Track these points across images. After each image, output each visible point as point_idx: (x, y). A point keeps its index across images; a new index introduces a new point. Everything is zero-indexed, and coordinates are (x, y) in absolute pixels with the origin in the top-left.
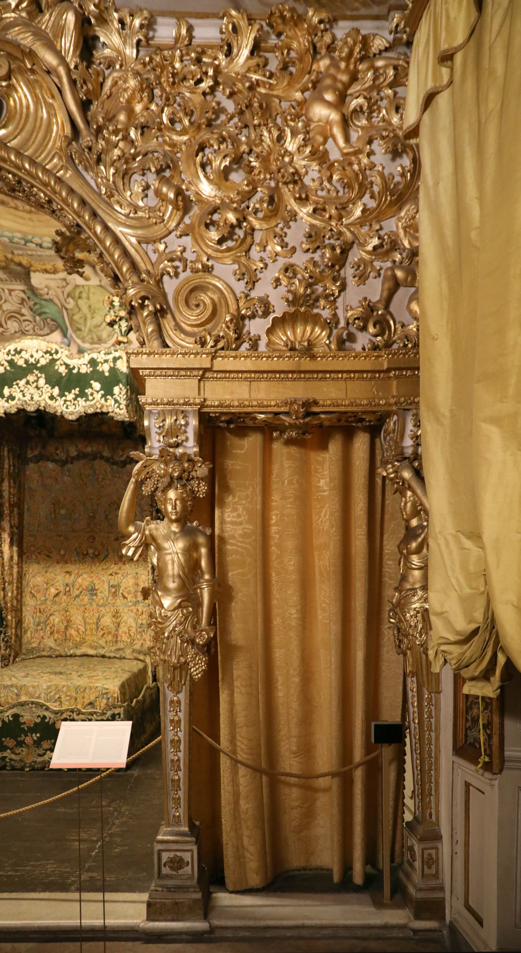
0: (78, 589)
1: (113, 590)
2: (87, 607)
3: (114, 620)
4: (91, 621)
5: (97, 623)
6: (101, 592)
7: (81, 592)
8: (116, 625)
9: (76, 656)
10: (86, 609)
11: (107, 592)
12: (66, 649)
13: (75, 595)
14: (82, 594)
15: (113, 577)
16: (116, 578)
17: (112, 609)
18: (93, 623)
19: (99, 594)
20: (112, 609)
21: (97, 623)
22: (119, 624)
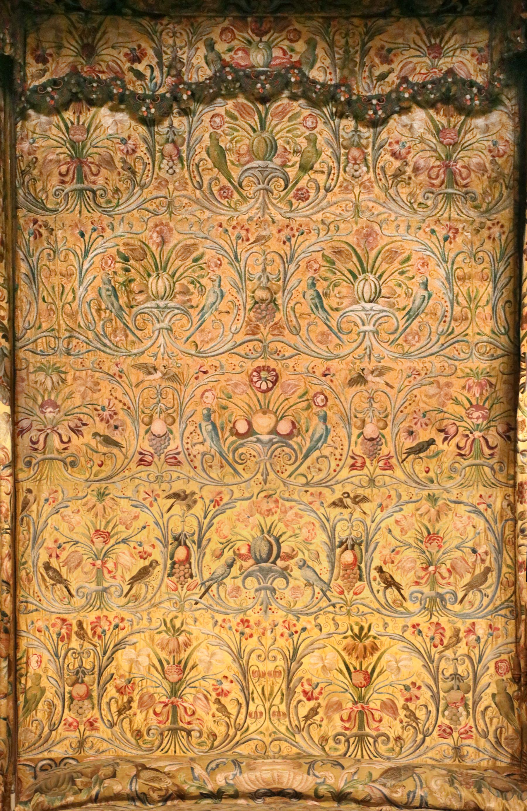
0: (219, 557)
1: (348, 557)
2: (253, 617)
3: (353, 662)
4: (269, 666)
5: (289, 674)
6: (304, 565)
7: (230, 566)
8: (359, 678)
9: (236, 795)
10: (245, 622)
11: (325, 564)
12: (199, 771)
13: (206, 576)
14: (235, 570)
15: (346, 513)
16: (357, 515)
17: (344, 622)
18: (276, 673)
19: (296, 572)
20: (344, 622)
21: (289, 674)
22: (369, 677)
